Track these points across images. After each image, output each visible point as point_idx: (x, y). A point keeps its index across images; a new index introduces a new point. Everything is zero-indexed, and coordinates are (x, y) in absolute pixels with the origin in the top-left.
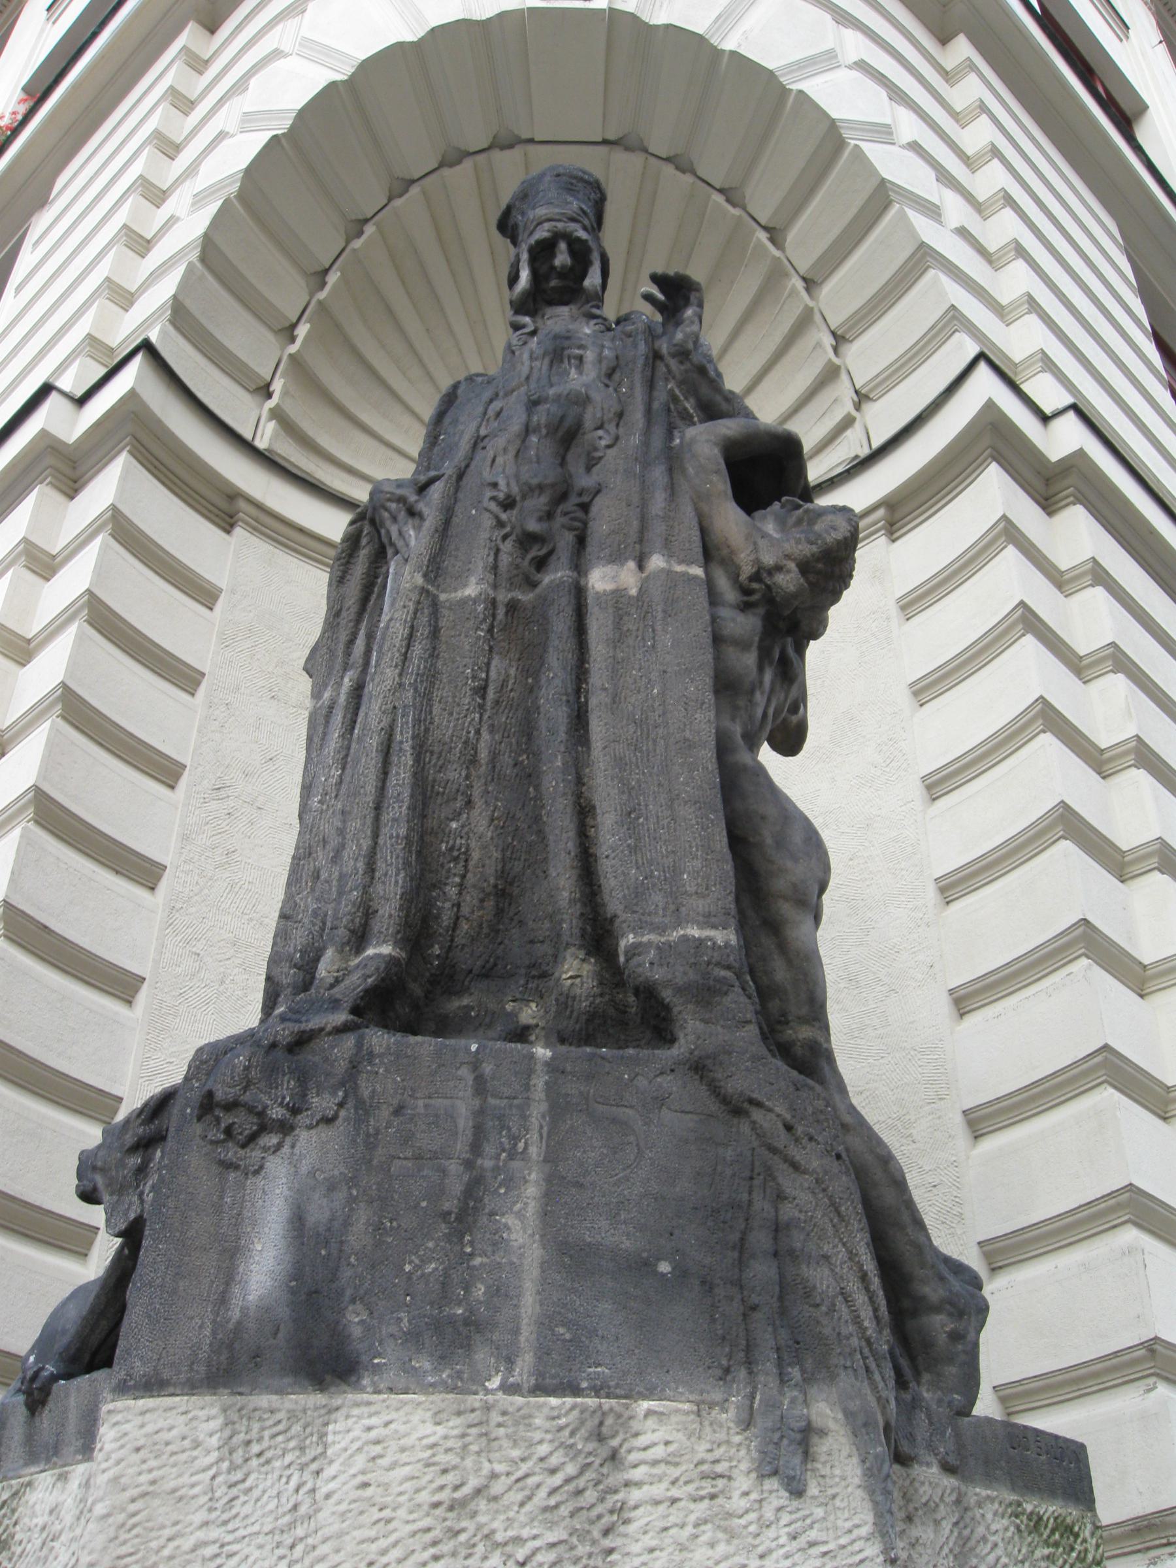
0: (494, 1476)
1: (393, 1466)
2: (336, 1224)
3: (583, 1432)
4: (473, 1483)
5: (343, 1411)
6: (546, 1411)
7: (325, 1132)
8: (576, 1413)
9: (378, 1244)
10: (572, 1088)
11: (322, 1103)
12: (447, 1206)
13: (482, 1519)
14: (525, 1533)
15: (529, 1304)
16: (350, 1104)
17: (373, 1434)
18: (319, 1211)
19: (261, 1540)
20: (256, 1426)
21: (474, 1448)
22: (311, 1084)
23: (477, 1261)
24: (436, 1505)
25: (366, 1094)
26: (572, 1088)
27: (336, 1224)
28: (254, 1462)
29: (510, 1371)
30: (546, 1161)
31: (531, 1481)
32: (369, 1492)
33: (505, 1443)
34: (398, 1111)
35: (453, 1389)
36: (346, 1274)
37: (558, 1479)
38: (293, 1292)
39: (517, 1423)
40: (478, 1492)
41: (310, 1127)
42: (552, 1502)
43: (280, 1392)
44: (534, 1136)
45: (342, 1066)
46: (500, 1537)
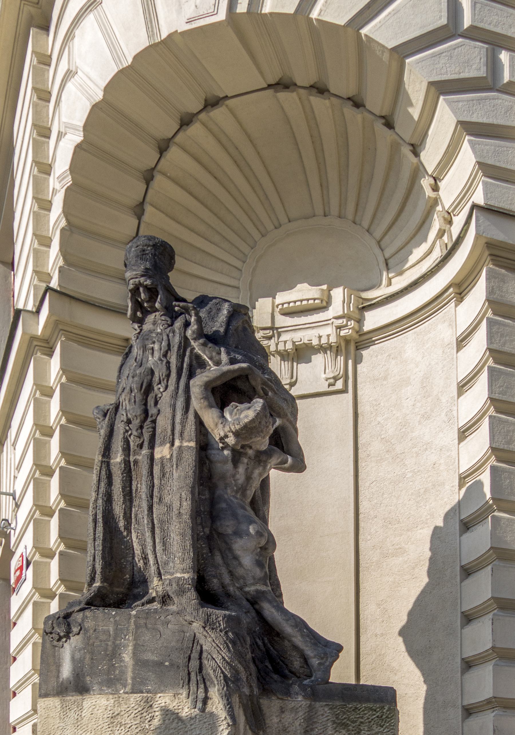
0: (121, 711)
1: (98, 710)
2: (82, 659)
3: (143, 701)
4: (116, 713)
5: (86, 699)
6: (133, 697)
7: (77, 637)
8: (141, 697)
9: (92, 663)
10: (142, 622)
11: (75, 630)
12: (108, 653)
13: (119, 720)
14: (129, 722)
15: (129, 675)
16: (83, 630)
17: (93, 704)
18: (78, 656)
19: (71, 725)
20: (67, 703)
21: (116, 706)
22: (72, 625)
23: (117, 665)
24: (108, 717)
25: (87, 627)
26: (142, 622)
27: (82, 659)
28: (68, 710)
29: (125, 689)
30: (134, 640)
31: (130, 712)
32: (93, 715)
33: (124, 704)
34: (95, 630)
35: (112, 694)
36: (85, 669)
37: (137, 711)
38: (73, 674)
39: (126, 700)
40: (118, 714)
41: (73, 636)
42: (136, 716)
43: (72, 696)
44: (131, 634)
45: (80, 621)
46: (123, 723)
